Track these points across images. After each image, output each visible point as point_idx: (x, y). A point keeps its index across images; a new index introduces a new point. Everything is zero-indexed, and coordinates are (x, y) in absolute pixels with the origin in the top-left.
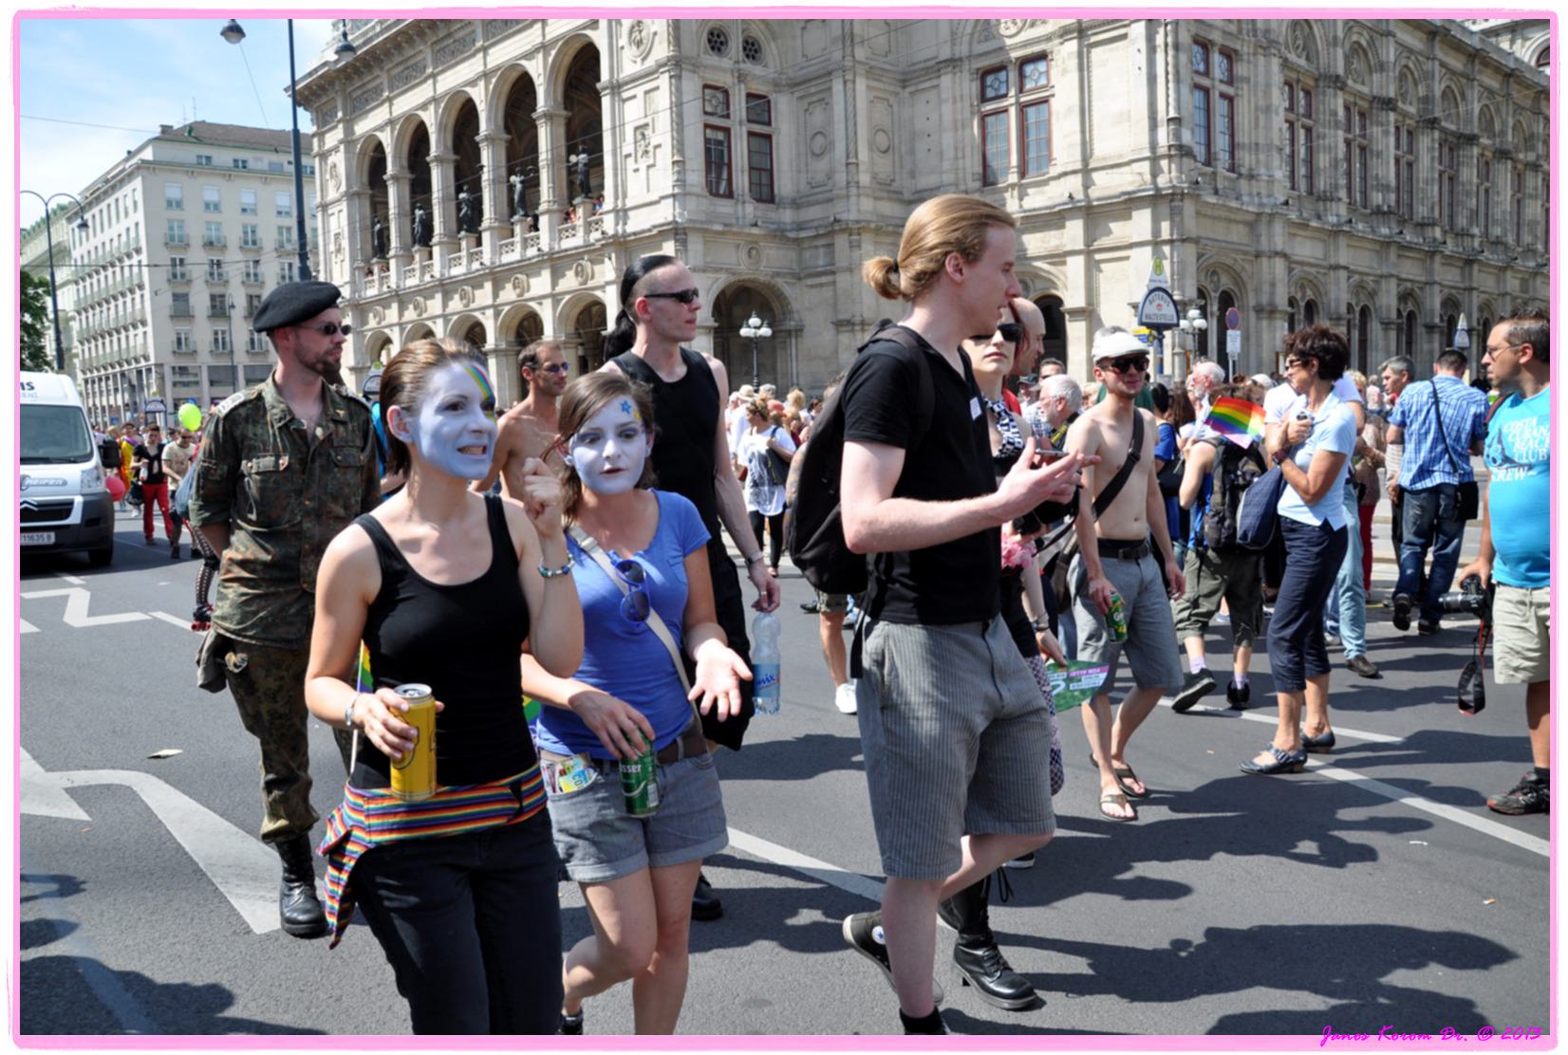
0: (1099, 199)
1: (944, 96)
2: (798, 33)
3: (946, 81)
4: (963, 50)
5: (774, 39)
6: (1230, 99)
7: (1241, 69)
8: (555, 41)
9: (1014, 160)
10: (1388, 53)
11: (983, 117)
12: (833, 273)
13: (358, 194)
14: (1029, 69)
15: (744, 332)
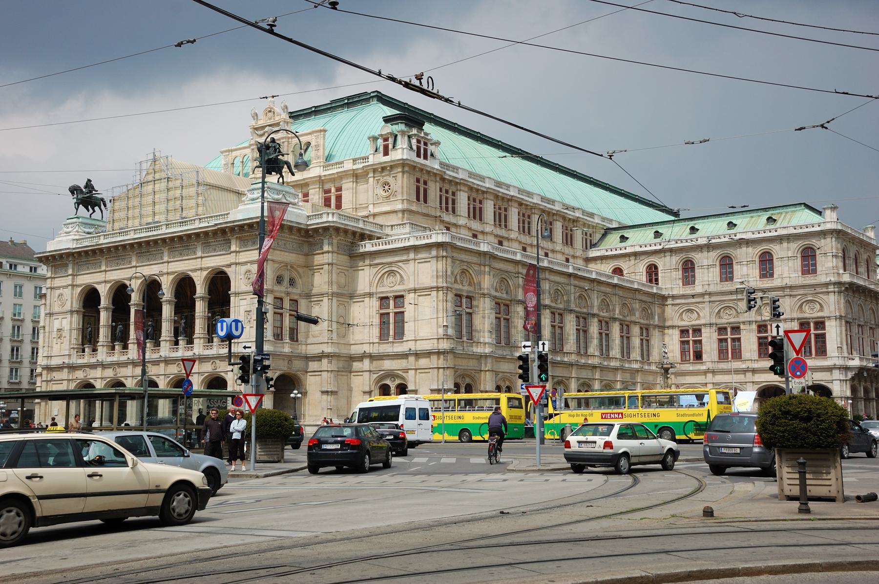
0: (420, 351)
1: (366, 305)
2: (310, 277)
3: (367, 300)
4: (373, 290)
5: (301, 277)
6: (470, 314)
7: (474, 303)
8: (208, 268)
9: (392, 332)
10: (546, 286)
11: (382, 315)
12: (321, 371)
13: (77, 312)
14: (397, 300)
15: (292, 395)
